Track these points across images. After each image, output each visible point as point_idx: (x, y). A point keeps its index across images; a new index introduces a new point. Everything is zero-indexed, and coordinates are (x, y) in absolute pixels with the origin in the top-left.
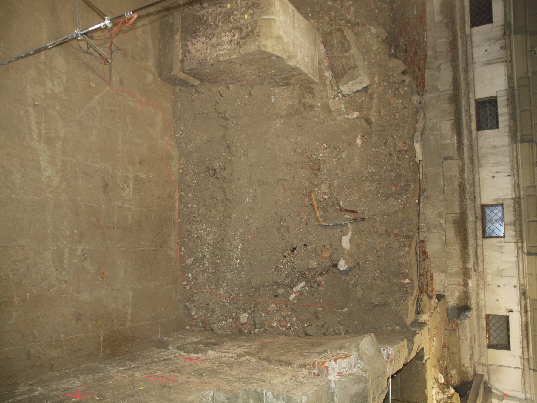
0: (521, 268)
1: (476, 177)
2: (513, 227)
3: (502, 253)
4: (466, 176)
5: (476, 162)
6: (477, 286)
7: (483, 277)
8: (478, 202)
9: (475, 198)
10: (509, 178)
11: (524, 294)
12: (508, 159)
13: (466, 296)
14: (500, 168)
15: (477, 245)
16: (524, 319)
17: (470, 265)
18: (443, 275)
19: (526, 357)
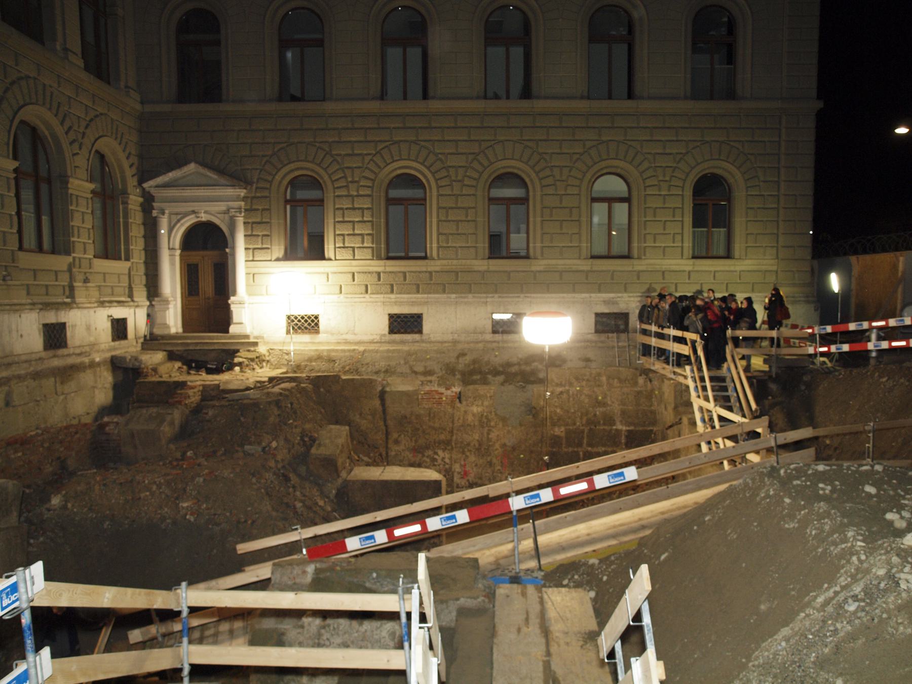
0: (89, 305)
1: (24, 358)
2: (59, 313)
3: (75, 325)
4: (23, 372)
5: (9, 360)
6: (98, 351)
7: (93, 345)
8: (43, 354)
9: (40, 359)
10: (23, 315)
11: (102, 304)
12: (6, 316)
13: (104, 362)
14: (14, 327)
15: (74, 354)
16: (115, 304)
17: (86, 360)
18: (97, 392)
19: (132, 304)
